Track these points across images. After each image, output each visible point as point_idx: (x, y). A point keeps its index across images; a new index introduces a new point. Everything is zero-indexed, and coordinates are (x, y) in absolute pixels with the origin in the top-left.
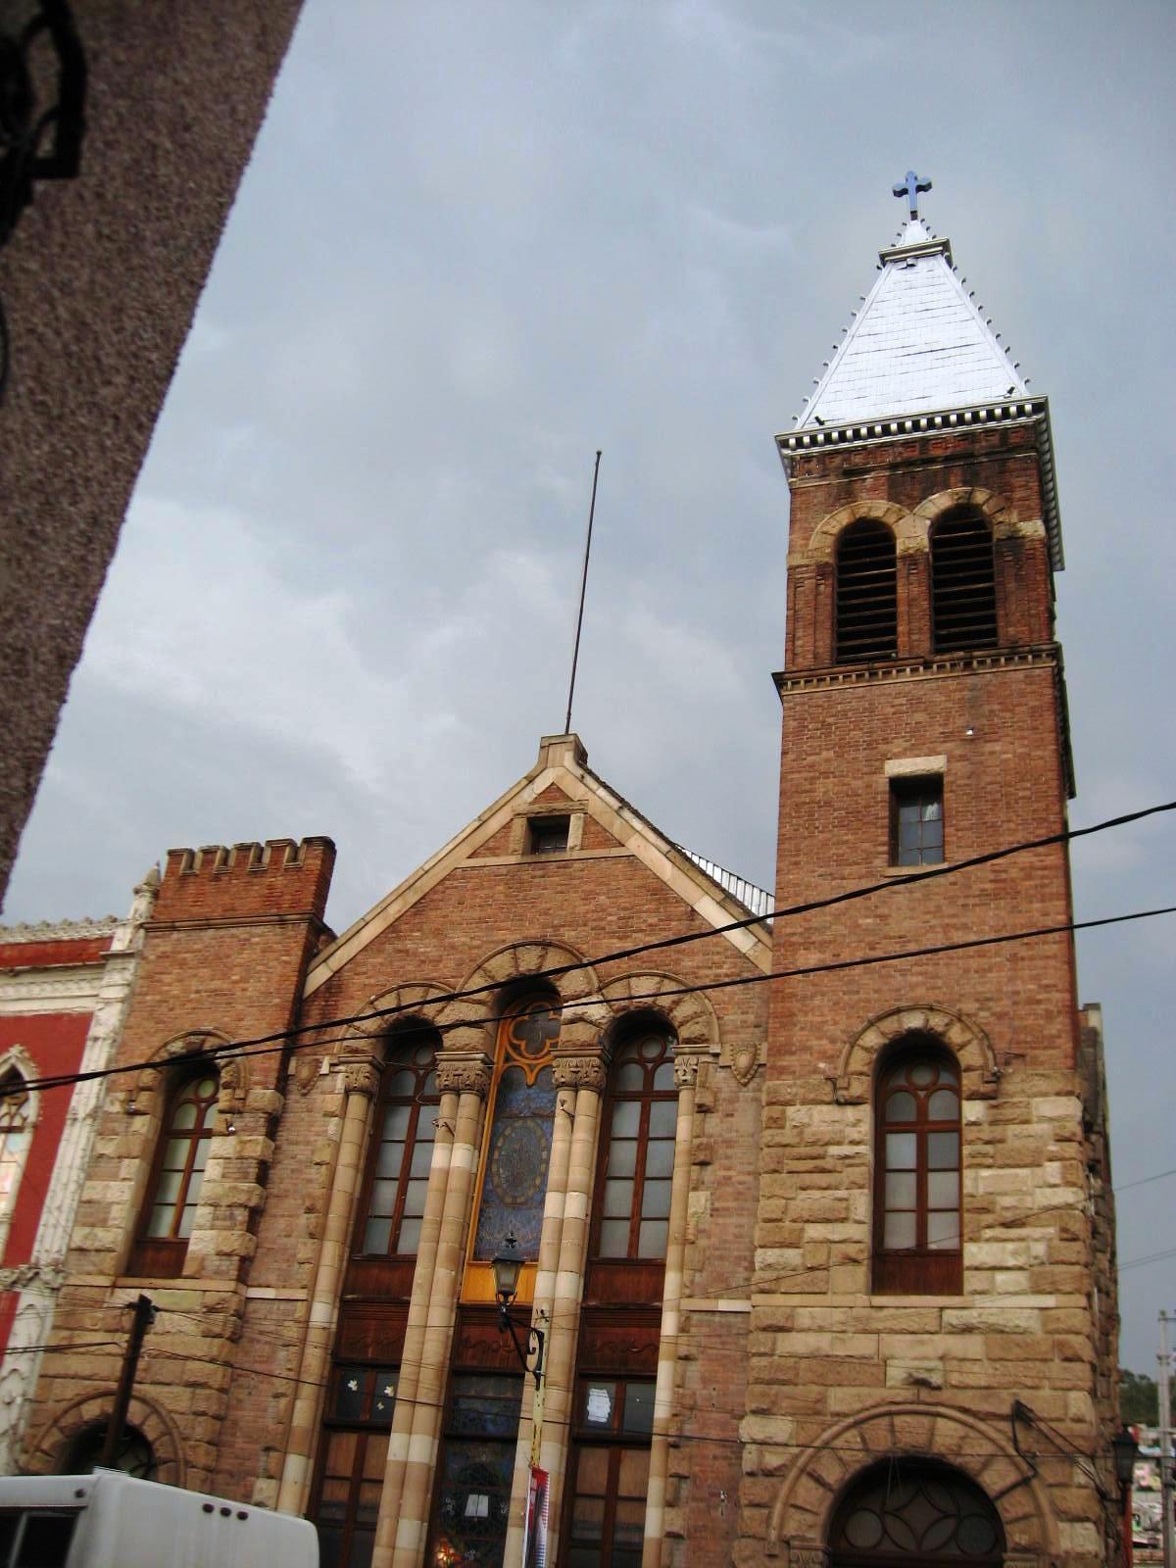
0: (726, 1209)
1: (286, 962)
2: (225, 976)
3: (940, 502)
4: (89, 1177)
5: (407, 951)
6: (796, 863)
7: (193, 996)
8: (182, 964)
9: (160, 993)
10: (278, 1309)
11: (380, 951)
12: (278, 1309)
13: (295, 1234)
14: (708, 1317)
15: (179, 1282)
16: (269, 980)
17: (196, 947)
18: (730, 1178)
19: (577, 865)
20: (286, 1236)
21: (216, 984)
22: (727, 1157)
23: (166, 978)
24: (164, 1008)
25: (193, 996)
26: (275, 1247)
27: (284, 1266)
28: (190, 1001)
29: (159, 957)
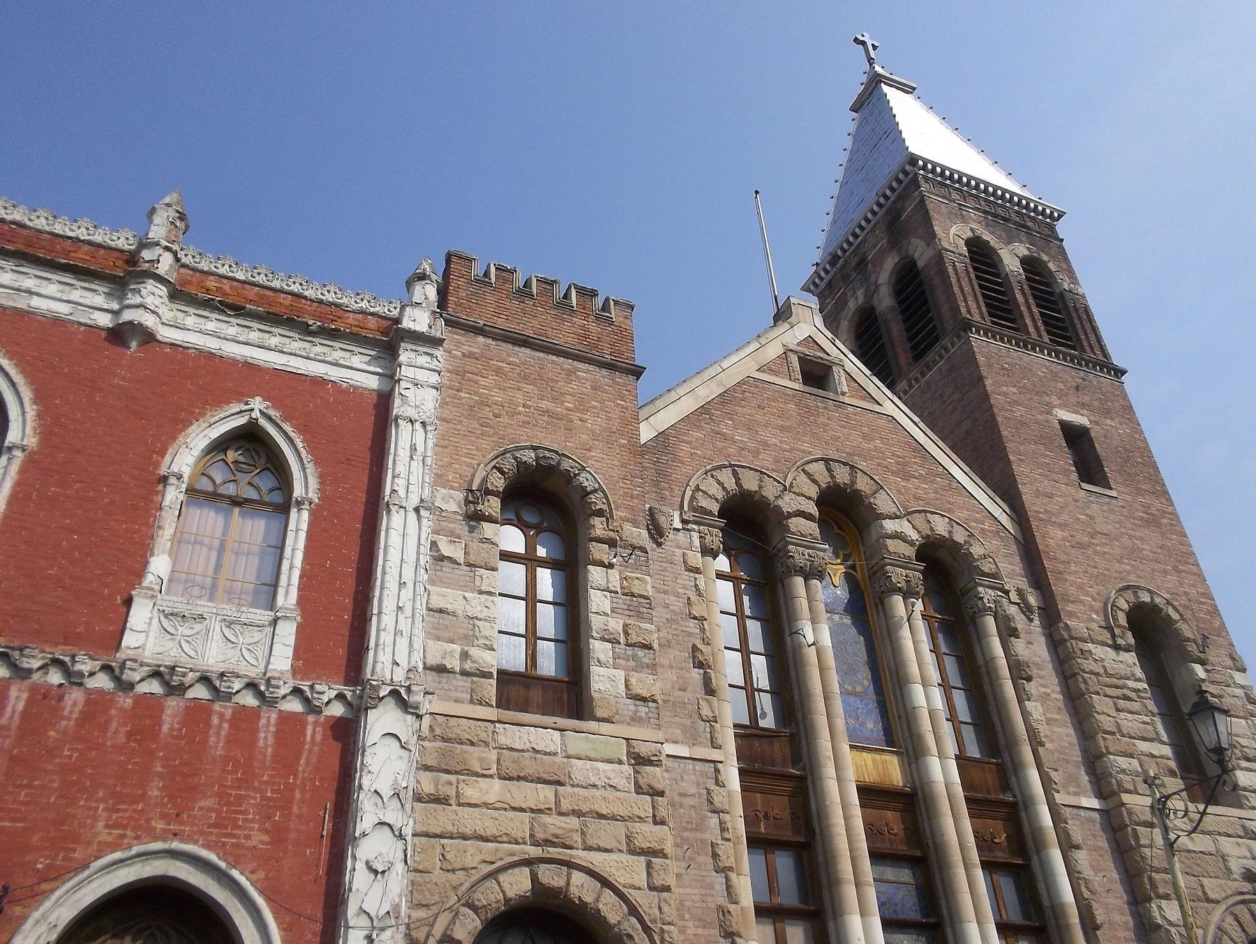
0: (1055, 720)
1: (623, 407)
2: (554, 400)
3: (1023, 250)
4: (432, 582)
5: (724, 435)
6: (1022, 460)
7: (521, 409)
8: (498, 372)
9: (476, 394)
10: (694, 769)
11: (700, 428)
12: (694, 769)
13: (690, 689)
14: (1076, 811)
15: (592, 725)
16: (609, 419)
17: (511, 359)
18: (1048, 695)
19: (850, 409)
20: (680, 690)
21: (545, 404)
22: (1040, 677)
23: (483, 382)
24: (487, 412)
25: (521, 409)
26: (672, 699)
27: (688, 722)
28: (520, 413)
29: (464, 355)
